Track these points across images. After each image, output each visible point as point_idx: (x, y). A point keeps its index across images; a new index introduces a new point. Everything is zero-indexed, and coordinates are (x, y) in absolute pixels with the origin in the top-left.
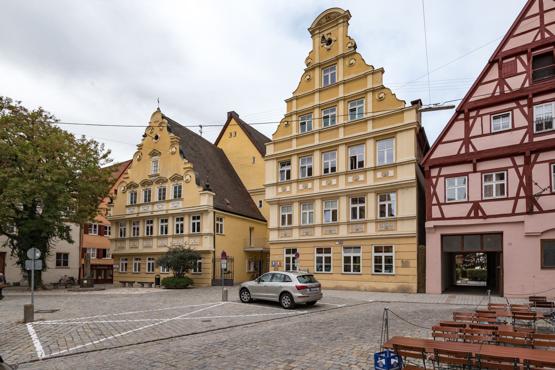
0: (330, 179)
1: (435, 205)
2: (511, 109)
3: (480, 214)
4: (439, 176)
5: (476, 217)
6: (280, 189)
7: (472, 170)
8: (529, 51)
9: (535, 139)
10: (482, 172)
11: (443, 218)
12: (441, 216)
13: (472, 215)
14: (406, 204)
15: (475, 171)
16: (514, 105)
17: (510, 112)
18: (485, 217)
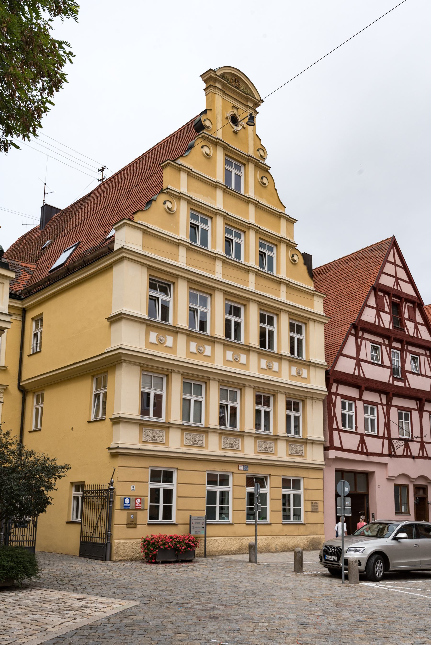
0: (238, 351)
1: (335, 430)
2: (380, 344)
3: (365, 451)
4: (336, 394)
5: (362, 453)
6: (153, 337)
7: (358, 397)
8: (392, 295)
9: (397, 383)
10: (366, 402)
11: (341, 449)
12: (340, 446)
13: (360, 450)
14: (313, 422)
15: (360, 399)
16: (380, 340)
17: (380, 346)
18: (367, 454)
